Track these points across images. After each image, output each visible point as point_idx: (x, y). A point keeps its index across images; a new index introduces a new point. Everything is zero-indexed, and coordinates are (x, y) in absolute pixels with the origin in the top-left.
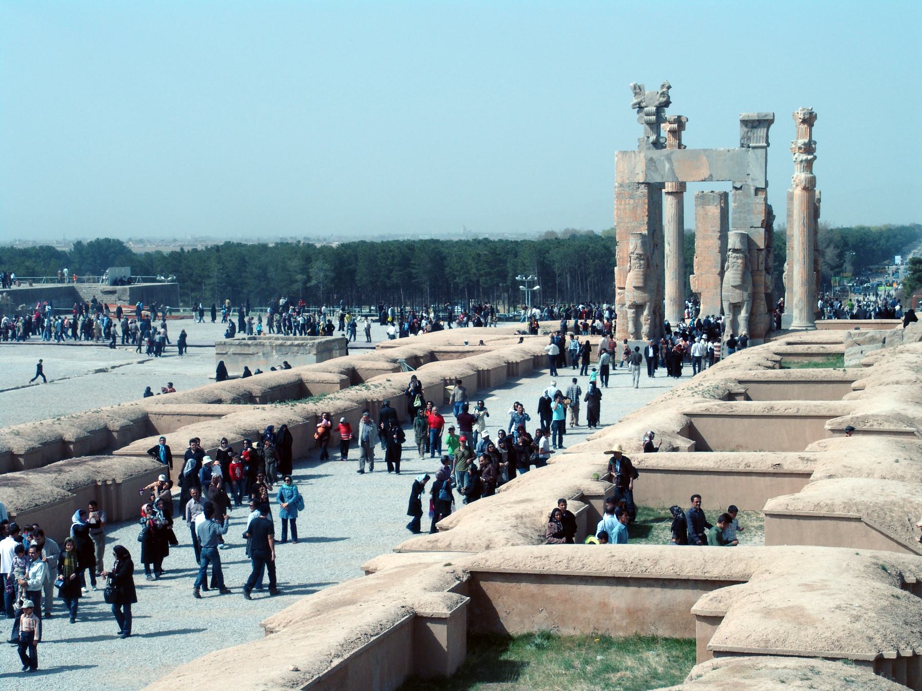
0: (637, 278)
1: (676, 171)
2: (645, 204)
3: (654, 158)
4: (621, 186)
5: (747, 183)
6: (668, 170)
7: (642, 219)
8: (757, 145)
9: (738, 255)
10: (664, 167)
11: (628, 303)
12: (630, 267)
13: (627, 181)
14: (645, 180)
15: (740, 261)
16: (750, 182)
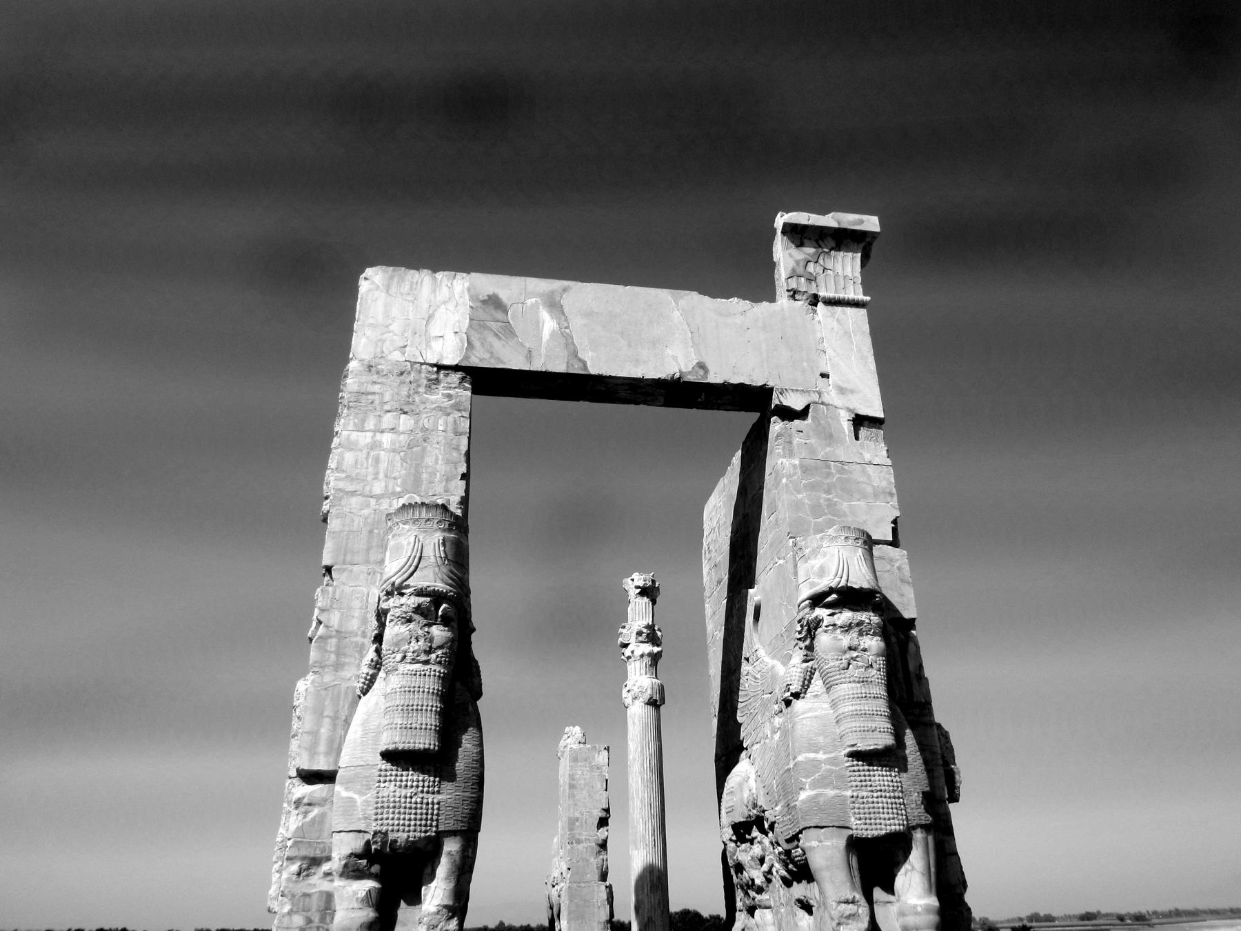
0: (408, 709)
1: (581, 343)
2: (457, 433)
3: (504, 296)
4: (370, 367)
5: (826, 399)
6: (553, 334)
7: (439, 488)
8: (841, 295)
10: (538, 325)
11: (343, 847)
12: (377, 665)
13: (397, 356)
14: (466, 358)
15: (874, 643)
16: (832, 397)
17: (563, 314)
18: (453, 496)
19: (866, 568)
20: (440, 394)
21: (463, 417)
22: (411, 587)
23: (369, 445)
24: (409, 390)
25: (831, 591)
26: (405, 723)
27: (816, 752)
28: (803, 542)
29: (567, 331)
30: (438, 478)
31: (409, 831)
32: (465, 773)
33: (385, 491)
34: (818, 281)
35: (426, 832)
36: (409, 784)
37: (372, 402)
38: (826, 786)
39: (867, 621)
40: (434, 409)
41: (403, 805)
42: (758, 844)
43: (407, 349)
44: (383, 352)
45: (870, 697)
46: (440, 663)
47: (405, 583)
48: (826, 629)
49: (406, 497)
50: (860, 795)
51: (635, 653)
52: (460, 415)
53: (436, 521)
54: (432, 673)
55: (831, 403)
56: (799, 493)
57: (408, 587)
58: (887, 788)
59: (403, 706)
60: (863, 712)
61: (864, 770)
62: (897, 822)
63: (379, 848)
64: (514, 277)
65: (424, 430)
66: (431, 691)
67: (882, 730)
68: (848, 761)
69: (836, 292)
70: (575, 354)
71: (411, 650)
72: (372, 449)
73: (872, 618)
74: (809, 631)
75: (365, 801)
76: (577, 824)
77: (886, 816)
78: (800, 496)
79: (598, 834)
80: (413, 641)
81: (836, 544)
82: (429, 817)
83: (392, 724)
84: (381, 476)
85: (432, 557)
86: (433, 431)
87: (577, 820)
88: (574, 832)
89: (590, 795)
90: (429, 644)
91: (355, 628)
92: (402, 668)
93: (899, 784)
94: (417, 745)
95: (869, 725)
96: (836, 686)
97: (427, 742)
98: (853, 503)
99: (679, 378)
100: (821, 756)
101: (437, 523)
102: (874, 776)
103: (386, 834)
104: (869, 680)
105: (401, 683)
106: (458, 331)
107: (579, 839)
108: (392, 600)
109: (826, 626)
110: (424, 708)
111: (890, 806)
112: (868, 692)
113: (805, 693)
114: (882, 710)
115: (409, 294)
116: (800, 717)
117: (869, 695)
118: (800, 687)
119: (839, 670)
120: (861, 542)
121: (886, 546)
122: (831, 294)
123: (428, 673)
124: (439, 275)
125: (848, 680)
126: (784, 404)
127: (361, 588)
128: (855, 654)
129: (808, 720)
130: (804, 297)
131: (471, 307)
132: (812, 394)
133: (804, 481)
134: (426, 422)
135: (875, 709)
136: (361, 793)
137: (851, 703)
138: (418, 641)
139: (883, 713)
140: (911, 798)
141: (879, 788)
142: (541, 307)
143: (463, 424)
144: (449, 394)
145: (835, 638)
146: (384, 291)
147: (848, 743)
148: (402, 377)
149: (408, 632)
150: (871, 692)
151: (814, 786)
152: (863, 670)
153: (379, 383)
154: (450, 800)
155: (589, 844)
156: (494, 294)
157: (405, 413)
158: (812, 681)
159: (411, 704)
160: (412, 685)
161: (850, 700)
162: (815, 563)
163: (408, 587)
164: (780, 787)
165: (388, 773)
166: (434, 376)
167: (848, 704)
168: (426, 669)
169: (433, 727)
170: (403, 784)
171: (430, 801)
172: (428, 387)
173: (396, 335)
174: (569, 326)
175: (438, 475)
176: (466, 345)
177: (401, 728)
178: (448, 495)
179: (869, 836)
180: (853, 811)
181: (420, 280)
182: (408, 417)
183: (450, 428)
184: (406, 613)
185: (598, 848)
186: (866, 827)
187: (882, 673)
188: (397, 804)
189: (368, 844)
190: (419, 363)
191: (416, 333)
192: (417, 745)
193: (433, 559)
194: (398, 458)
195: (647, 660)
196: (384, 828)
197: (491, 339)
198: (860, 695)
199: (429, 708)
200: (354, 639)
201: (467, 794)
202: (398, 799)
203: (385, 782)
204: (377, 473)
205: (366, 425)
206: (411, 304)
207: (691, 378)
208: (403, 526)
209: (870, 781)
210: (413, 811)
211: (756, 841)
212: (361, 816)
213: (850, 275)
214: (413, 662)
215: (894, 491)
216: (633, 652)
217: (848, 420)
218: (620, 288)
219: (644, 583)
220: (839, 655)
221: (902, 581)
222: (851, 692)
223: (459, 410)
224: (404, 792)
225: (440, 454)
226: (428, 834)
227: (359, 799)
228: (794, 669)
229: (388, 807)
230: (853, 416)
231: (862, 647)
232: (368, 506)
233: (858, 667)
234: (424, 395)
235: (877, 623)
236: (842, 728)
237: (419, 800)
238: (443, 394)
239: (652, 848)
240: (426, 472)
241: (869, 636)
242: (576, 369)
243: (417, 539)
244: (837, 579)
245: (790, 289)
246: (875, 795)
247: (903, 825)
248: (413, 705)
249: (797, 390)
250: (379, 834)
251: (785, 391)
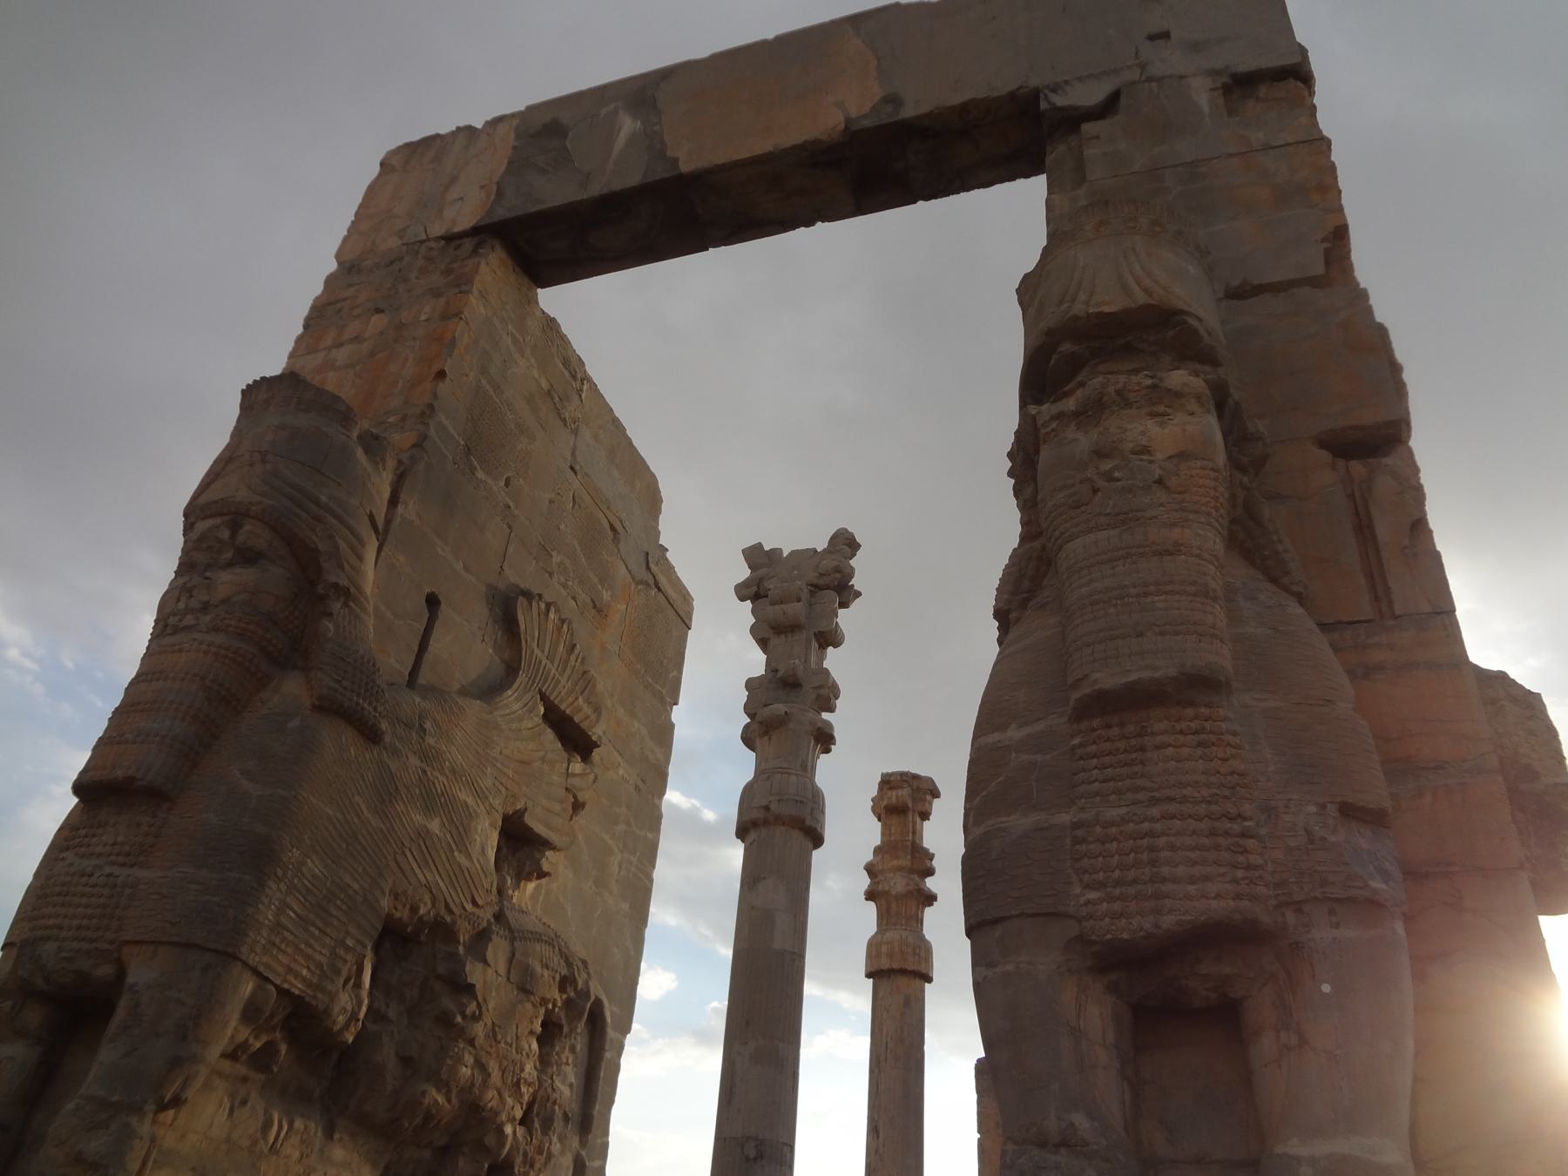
13: (393, 243)
21: (460, 292)
37: (340, 310)
39: (1149, 382)
157: (378, 311)
176: (493, 197)
179: (1125, 936)
182: (382, 316)
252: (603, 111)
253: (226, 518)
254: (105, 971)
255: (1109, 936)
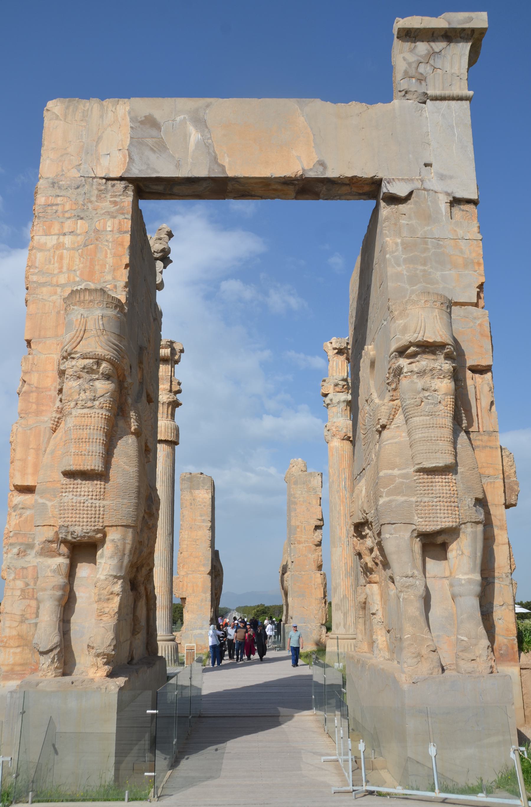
2: (121, 231)
3: (158, 115)
6: (197, 144)
7: (109, 277)
8: (447, 92)
9: (437, 365)
10: (186, 137)
13: (74, 173)
14: (128, 170)
16: (433, 183)
17: (207, 127)
18: (119, 282)
19: (440, 326)
20: (108, 202)
21: (126, 218)
22: (79, 352)
23: (55, 246)
24: (84, 200)
25: (411, 344)
26: (77, 451)
27: (393, 469)
28: (394, 306)
29: (210, 141)
30: (107, 269)
31: (83, 526)
32: (123, 486)
33: (68, 281)
34: (428, 80)
35: (95, 526)
36: (82, 493)
37: (56, 212)
38: (398, 494)
39: (439, 368)
40: (104, 214)
41: (78, 508)
42: (370, 539)
43: (82, 167)
44: (63, 171)
45: (437, 427)
46: (102, 408)
47: (74, 350)
48: (406, 374)
49: (84, 284)
50: (423, 501)
51: (334, 401)
52: (124, 217)
53: (96, 302)
54: (96, 415)
55: (432, 188)
56: (399, 265)
57: (76, 353)
58: (445, 495)
59: (75, 439)
60: (429, 438)
61: (428, 482)
62: (450, 520)
63: (64, 537)
64: (166, 98)
65: (97, 231)
66: (96, 428)
67: (443, 452)
68: (416, 475)
69: (443, 90)
70: (215, 159)
71: (81, 398)
72: (57, 249)
73: (443, 365)
74: (395, 376)
75: (52, 505)
76: (298, 530)
77: (442, 515)
78: (399, 269)
79: (314, 537)
80: (82, 392)
81: (417, 307)
82: (97, 516)
83: (67, 452)
84: (65, 269)
85: (93, 330)
86: (103, 231)
87: (298, 527)
88: (295, 536)
89: (308, 509)
90: (94, 395)
91: (49, 384)
92: (75, 412)
93: (456, 492)
94: (85, 467)
95: (434, 449)
96: (411, 419)
97: (93, 465)
98: (445, 272)
99: (302, 175)
100: (396, 472)
101: (97, 303)
102: (436, 486)
103: (67, 527)
104: (437, 413)
105: (75, 423)
106: (121, 148)
107: (299, 541)
108: (66, 363)
109: (406, 373)
110: (91, 440)
111: (446, 508)
112: (435, 423)
113: (390, 424)
114: (445, 436)
115: (82, 120)
116: (384, 443)
117: (435, 426)
118: (386, 421)
119: (413, 407)
120: (438, 304)
121: (471, 307)
122: (438, 92)
123: (93, 415)
124: (105, 103)
125: (419, 414)
126: (391, 192)
127: (53, 355)
128: (427, 394)
129: (389, 445)
130: (415, 96)
131: (132, 127)
132: (415, 182)
133: (404, 256)
134: (99, 226)
135: (439, 436)
136: (50, 500)
137: (421, 432)
138: (85, 392)
139: (446, 439)
140: (465, 502)
141: (438, 495)
142: (188, 123)
143: (126, 225)
144: (115, 201)
145: (412, 382)
146: (63, 119)
147: (416, 462)
148: (79, 190)
149: (78, 386)
150: (438, 423)
151: (388, 494)
152: (433, 406)
153: (61, 196)
154: (112, 505)
155: (307, 545)
156: (150, 114)
157: (82, 219)
158: (397, 416)
159: (81, 438)
160: (82, 425)
161: (420, 429)
162: (401, 322)
163: (76, 353)
164: (374, 496)
165: (68, 486)
166: (103, 187)
167: (418, 432)
168: (92, 413)
169: (97, 454)
170: (78, 493)
171: (97, 505)
172: (98, 197)
173: (72, 156)
174: (211, 137)
175: (107, 266)
176: (128, 160)
177: (74, 455)
178: (115, 282)
179: (428, 530)
180: (416, 512)
181: (90, 109)
182: (84, 222)
183: (116, 226)
184: (76, 372)
185: (314, 547)
186: (426, 523)
187: (449, 409)
188: (75, 508)
189: (56, 532)
190: (91, 177)
191: (88, 153)
192: (85, 467)
193: (94, 332)
194: (77, 255)
195: (343, 406)
196: (66, 524)
197: (148, 153)
198: (428, 426)
199: (94, 440)
200: (49, 393)
201: (125, 501)
202: (75, 504)
203: (66, 492)
204: (61, 268)
205: (52, 230)
206: (84, 128)
207: (312, 174)
208: (73, 307)
209: (432, 490)
210: (86, 512)
211: (368, 536)
212: (51, 516)
213: (457, 72)
214: (82, 407)
215: (482, 261)
216: (331, 400)
217: (446, 203)
218: (254, 102)
219: (340, 345)
220: (414, 395)
221: (482, 335)
222: (421, 424)
223: (123, 214)
224: (79, 499)
225: (109, 249)
226: (96, 528)
227: (49, 504)
228: (383, 407)
229: (68, 509)
230: (452, 199)
231: (433, 388)
232: (55, 293)
233: (428, 404)
234: (96, 203)
235: (449, 370)
236: (413, 451)
237: (89, 505)
238: (110, 202)
239: (347, 546)
240: (98, 265)
241: (440, 380)
242: (217, 174)
243: (83, 316)
244: (416, 335)
245: (402, 90)
246: (435, 500)
247: (456, 522)
248: (82, 439)
249: (402, 179)
250: (63, 528)
251: (392, 180)
252: (178, 119)
253: (94, 360)
254: (99, 535)
255: (424, 530)
